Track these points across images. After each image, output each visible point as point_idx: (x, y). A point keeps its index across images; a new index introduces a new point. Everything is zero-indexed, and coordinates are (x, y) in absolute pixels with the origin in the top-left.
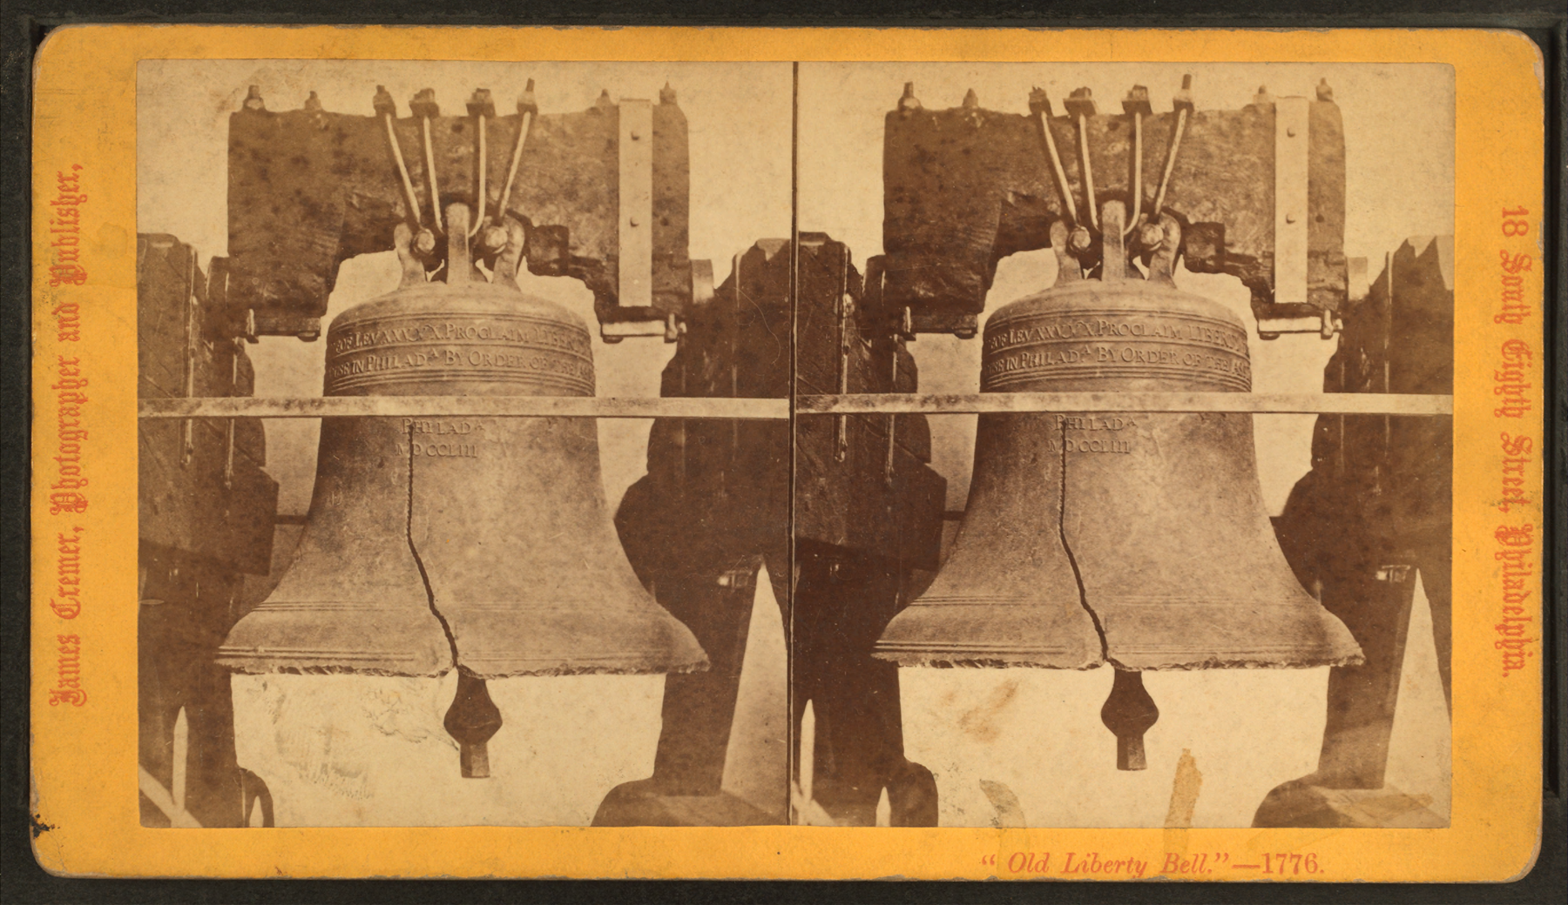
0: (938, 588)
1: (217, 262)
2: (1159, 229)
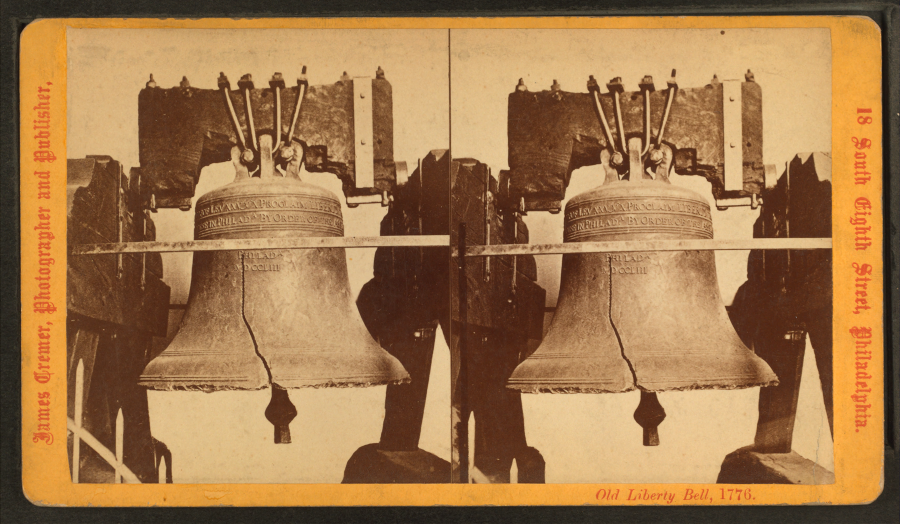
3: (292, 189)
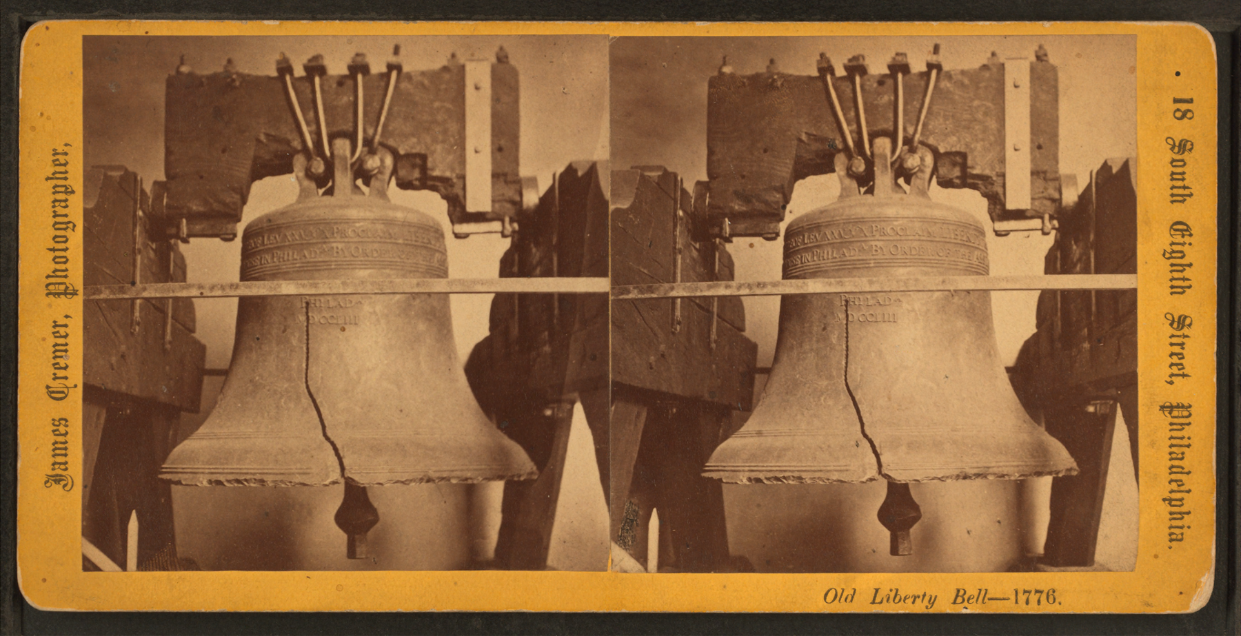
0: (751, 425)
1: (156, 183)
2: (917, 157)
3: (376, 213)
